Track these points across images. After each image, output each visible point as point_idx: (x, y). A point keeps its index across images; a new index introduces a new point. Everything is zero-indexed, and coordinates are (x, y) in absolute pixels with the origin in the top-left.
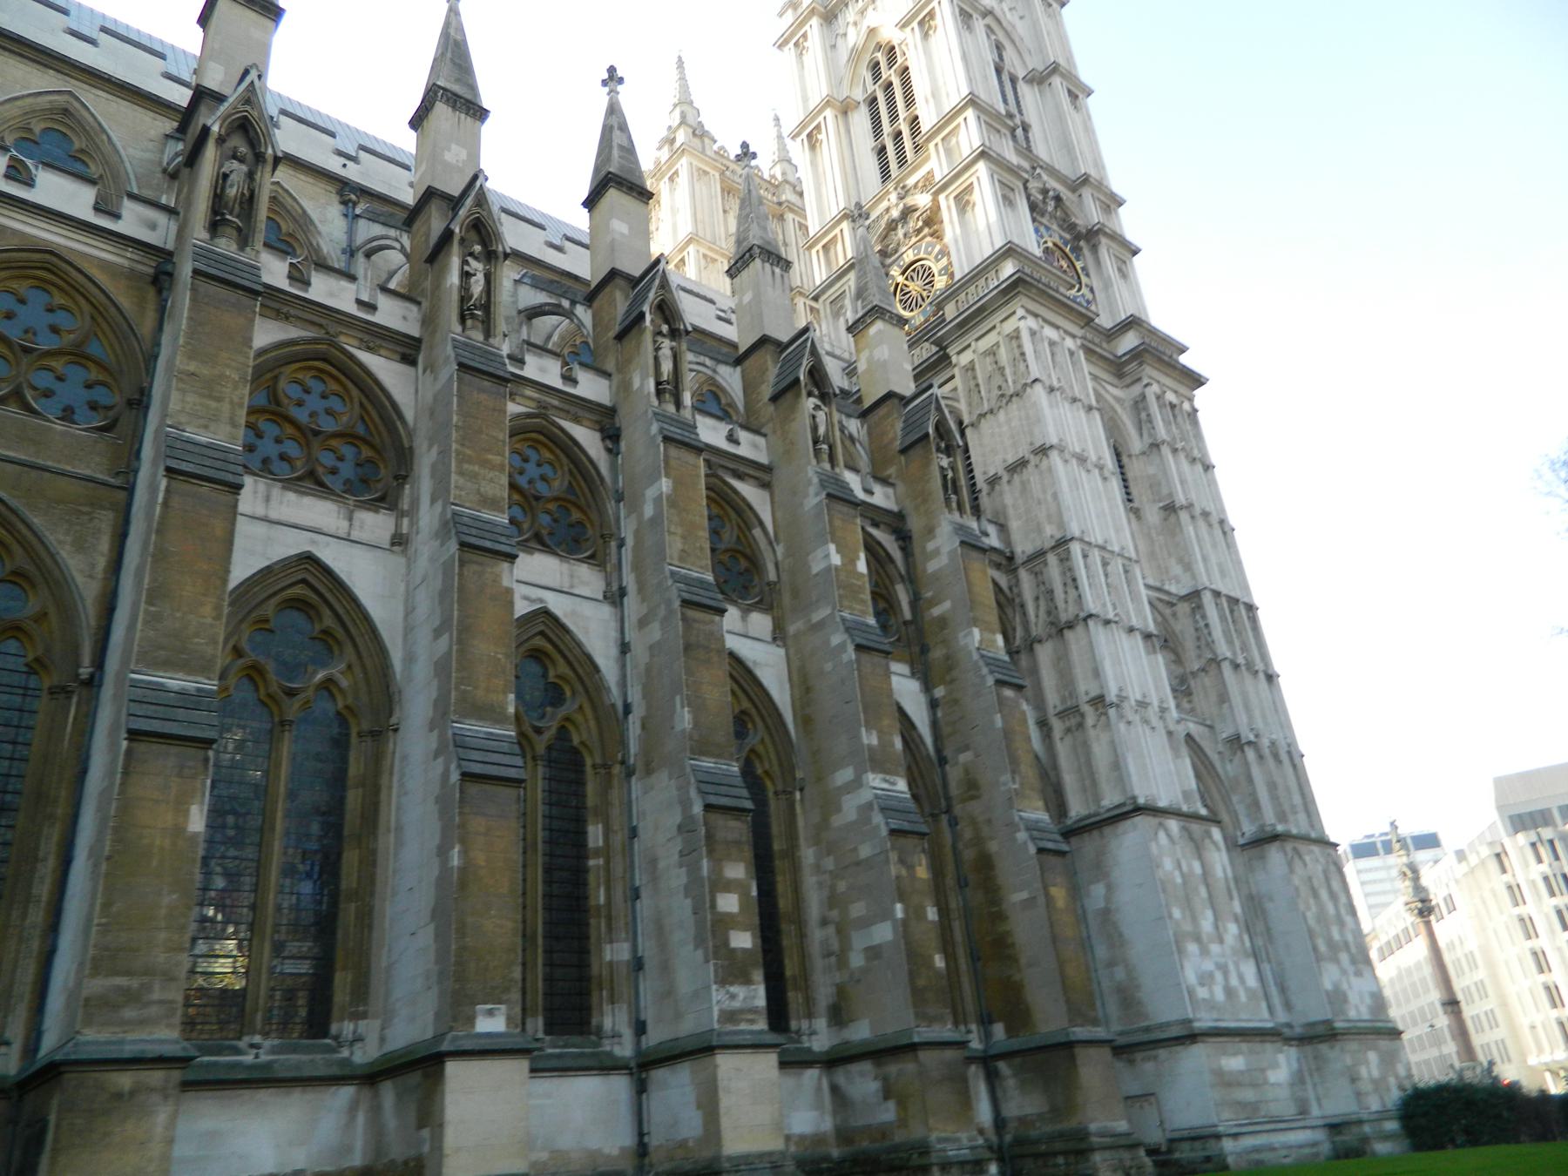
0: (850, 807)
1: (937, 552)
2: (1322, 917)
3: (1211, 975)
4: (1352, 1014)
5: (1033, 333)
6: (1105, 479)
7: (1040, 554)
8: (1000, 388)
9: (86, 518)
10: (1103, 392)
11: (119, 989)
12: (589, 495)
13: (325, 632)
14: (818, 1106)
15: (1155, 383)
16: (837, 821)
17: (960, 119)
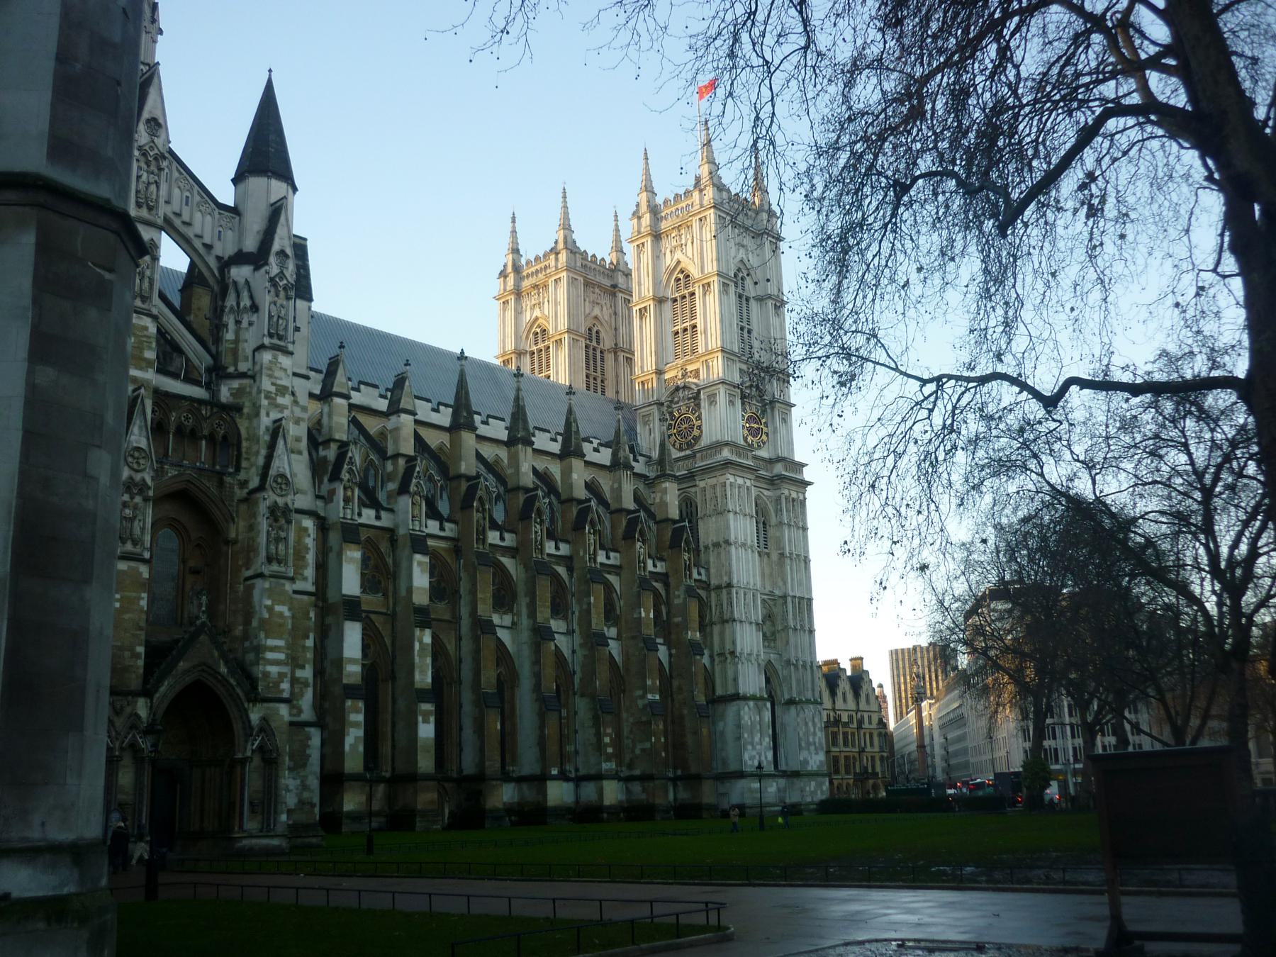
2: (807, 733)
4: (809, 768)
5: (731, 484)
17: (715, 355)
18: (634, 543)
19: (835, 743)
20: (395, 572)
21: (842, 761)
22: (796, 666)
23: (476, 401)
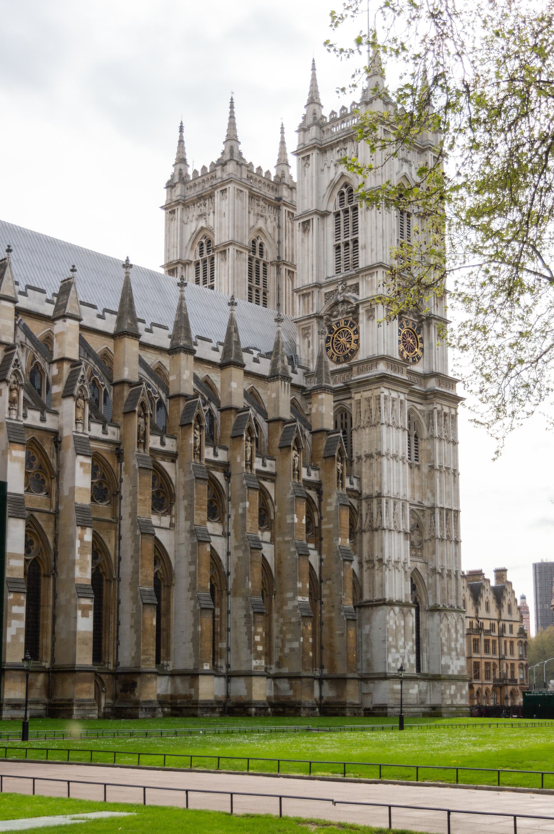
0: (290, 605)
1: (331, 504)
2: (449, 640)
3: (398, 659)
4: (450, 673)
5: (386, 398)
6: (404, 463)
14: (270, 689)
16: (285, 608)
18: (289, 451)
19: (476, 650)
20: (59, 472)
21: (483, 668)
22: (441, 574)
23: (140, 310)
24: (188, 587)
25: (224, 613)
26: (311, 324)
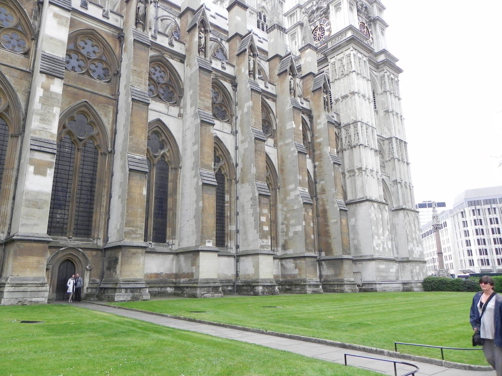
0: (292, 195)
1: (320, 123)
3: (380, 244)
4: (414, 256)
5: (354, 55)
7: (348, 125)
8: (342, 71)
9: (106, 107)
10: (372, 74)
11: (131, 230)
12: (228, 103)
13: (163, 140)
14: (278, 268)
15: (387, 72)
16: (288, 198)
24: (192, 165)
25: (234, 199)
26: (296, 31)
